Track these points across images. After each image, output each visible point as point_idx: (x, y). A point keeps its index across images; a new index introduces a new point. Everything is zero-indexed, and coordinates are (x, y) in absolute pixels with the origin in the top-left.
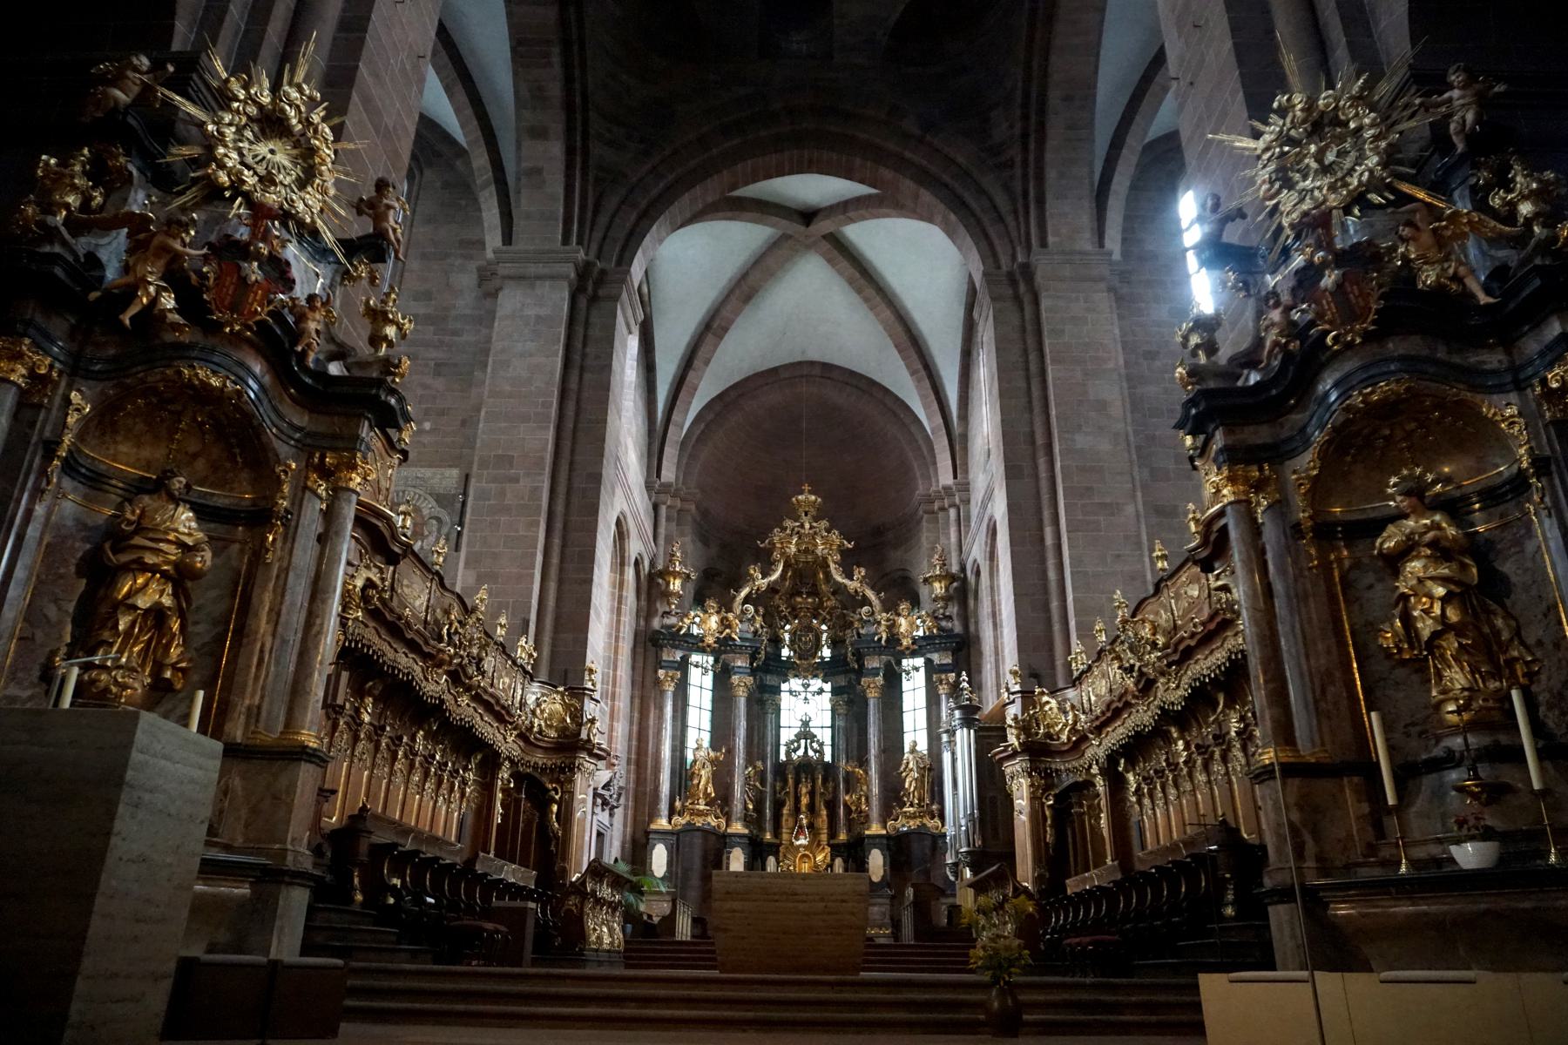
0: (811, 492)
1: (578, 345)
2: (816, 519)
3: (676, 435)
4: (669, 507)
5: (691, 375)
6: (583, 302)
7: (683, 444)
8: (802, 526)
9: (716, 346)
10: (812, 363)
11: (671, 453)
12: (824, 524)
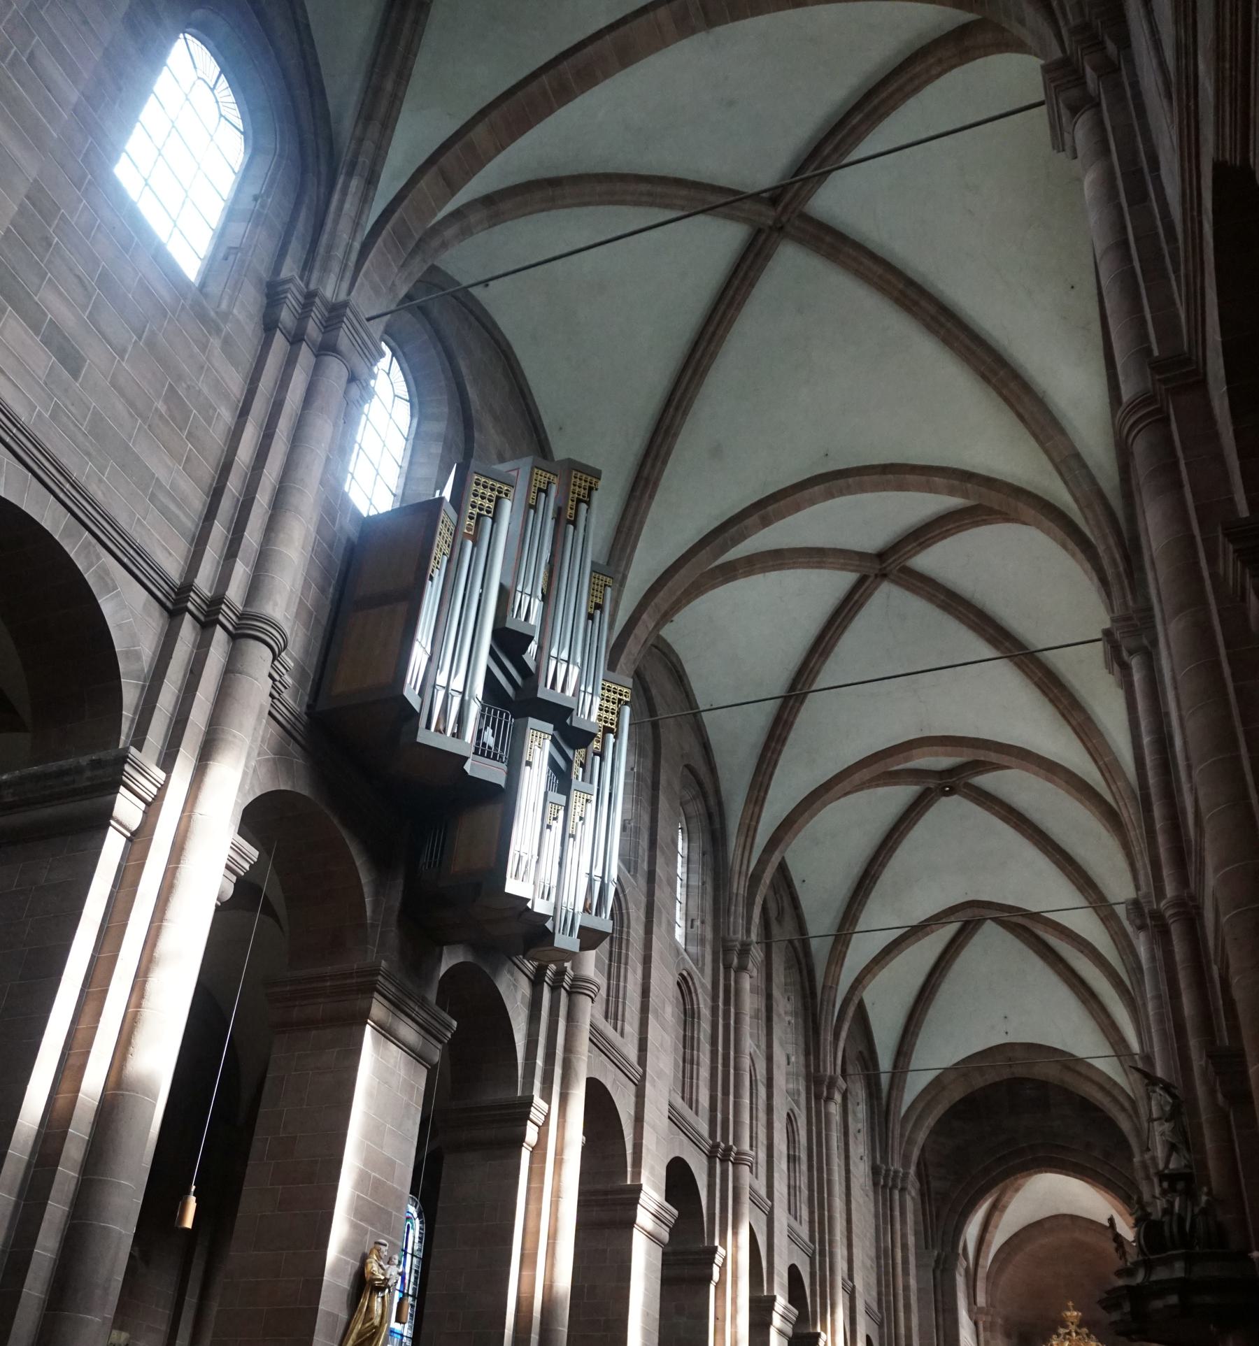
0: (1075, 1309)
1: (940, 1298)
2: (1080, 1326)
3: (982, 1274)
4: (984, 1322)
5: (988, 1236)
6: (938, 1273)
7: (988, 1277)
8: (1069, 1334)
9: (1001, 1217)
10: (1064, 1216)
11: (981, 1285)
12: (1085, 1330)
